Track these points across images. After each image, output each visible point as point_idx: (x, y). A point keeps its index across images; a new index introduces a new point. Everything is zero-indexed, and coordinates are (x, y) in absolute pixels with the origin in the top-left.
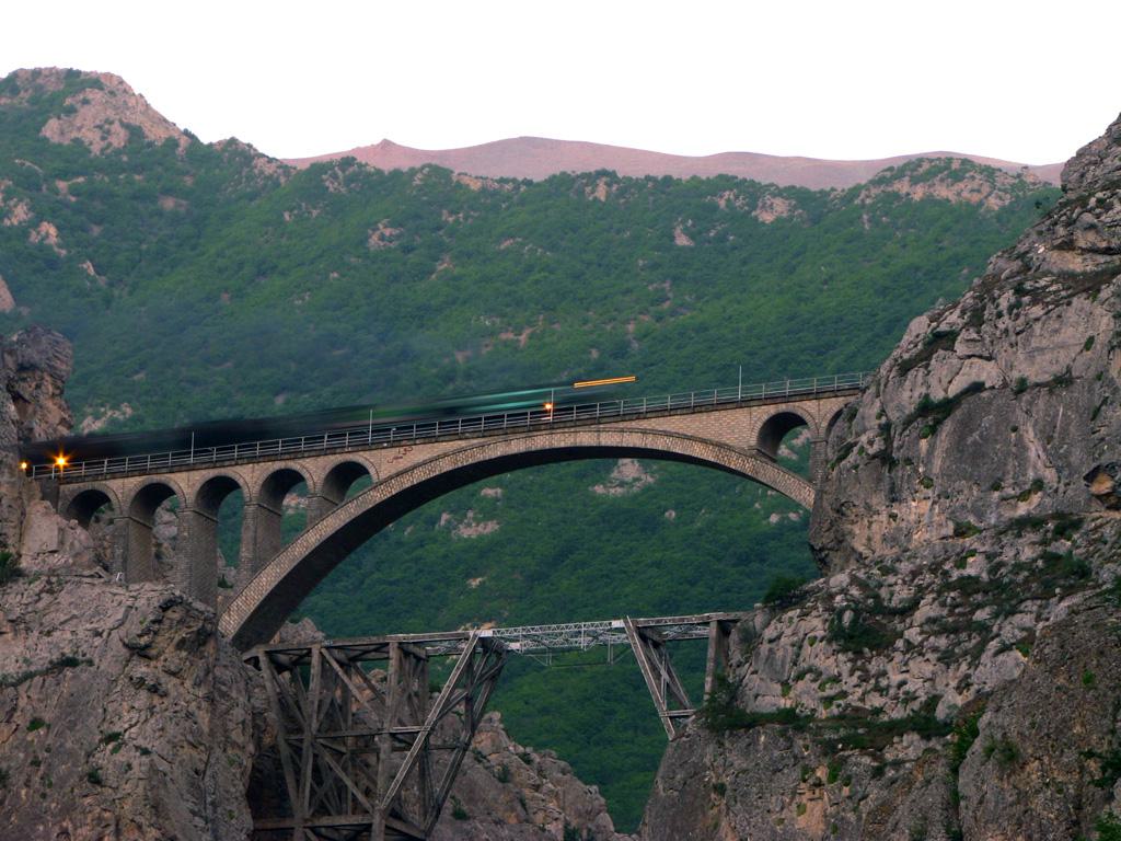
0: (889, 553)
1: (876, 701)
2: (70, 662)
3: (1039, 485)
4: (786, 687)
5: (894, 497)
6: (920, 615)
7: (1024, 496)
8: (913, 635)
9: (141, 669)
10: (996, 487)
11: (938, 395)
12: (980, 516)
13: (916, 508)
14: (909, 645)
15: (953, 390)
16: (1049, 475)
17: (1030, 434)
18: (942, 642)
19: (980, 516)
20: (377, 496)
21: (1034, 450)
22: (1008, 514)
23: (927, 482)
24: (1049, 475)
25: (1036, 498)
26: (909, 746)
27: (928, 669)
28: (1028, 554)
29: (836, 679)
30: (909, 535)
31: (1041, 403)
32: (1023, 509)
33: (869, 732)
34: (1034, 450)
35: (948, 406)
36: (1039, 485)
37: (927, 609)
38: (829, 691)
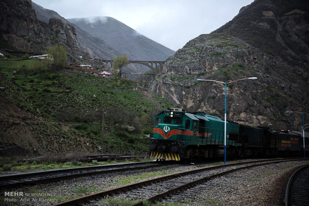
35: (174, 67)
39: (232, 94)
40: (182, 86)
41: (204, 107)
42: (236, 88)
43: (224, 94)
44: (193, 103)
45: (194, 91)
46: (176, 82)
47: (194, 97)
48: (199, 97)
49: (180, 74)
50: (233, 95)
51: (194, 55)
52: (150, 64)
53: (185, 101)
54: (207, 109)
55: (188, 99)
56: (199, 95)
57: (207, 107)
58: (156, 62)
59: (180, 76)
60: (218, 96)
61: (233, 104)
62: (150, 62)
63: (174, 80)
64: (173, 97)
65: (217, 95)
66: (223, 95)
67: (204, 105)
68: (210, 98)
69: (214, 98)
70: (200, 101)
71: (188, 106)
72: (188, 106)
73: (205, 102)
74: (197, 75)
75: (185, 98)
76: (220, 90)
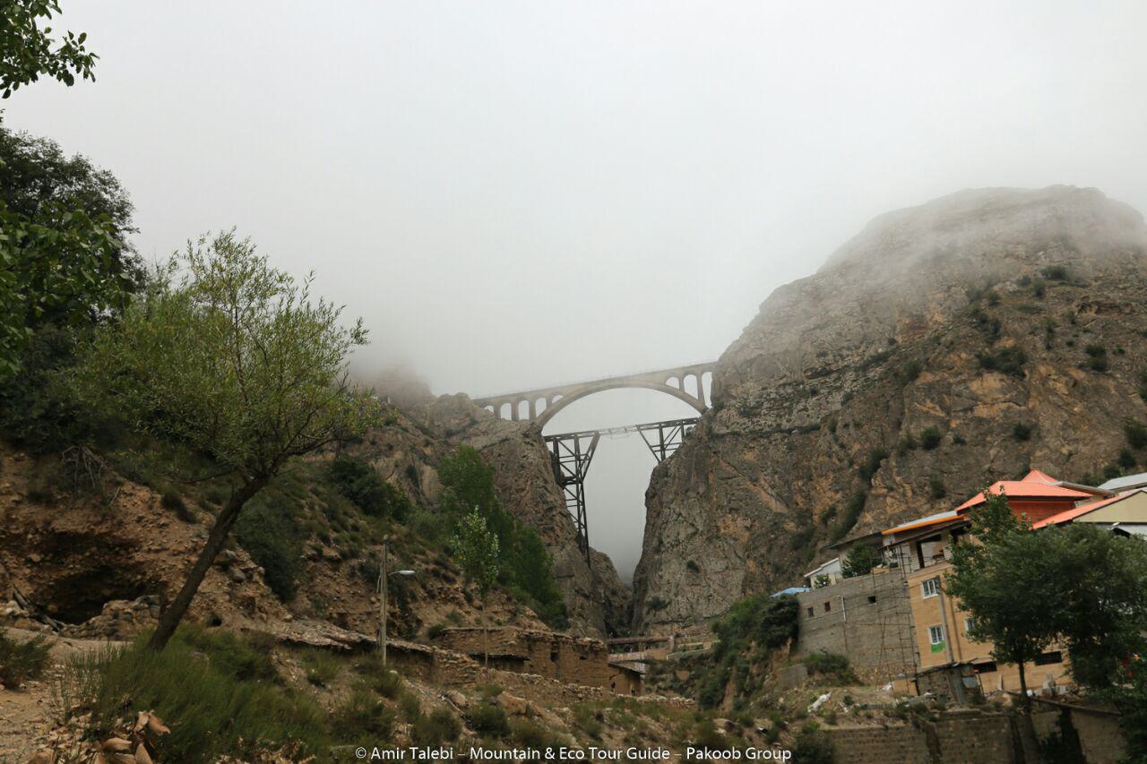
1: (757, 428)
2: (507, 439)
3: (785, 376)
4: (728, 427)
5: (742, 382)
7: (781, 379)
8: (765, 411)
9: (528, 440)
10: (772, 377)
12: (769, 384)
14: (765, 415)
15: (753, 356)
16: (788, 374)
18: (775, 412)
19: (769, 384)
24: (788, 374)
25: (784, 380)
26: (778, 436)
27: (773, 419)
28: (790, 391)
29: (744, 424)
32: (781, 382)
33: (758, 435)
37: (766, 405)
38: (744, 426)
39: (1025, 404)
40: (790, 431)
41: (889, 500)
42: (1043, 369)
43: (982, 411)
44: (837, 491)
46: (767, 421)
47: (835, 460)
49: (784, 385)
50: (1031, 411)
51: (834, 292)
52: (673, 382)
53: (800, 490)
54: (904, 507)
57: (904, 495)
59: (782, 391)
61: (1038, 454)
62: (670, 373)
63: (755, 415)
64: (755, 490)
65: (946, 424)
66: (980, 420)
68: (910, 445)
70: (867, 474)
73: (888, 469)
74: (856, 370)
75: (798, 478)
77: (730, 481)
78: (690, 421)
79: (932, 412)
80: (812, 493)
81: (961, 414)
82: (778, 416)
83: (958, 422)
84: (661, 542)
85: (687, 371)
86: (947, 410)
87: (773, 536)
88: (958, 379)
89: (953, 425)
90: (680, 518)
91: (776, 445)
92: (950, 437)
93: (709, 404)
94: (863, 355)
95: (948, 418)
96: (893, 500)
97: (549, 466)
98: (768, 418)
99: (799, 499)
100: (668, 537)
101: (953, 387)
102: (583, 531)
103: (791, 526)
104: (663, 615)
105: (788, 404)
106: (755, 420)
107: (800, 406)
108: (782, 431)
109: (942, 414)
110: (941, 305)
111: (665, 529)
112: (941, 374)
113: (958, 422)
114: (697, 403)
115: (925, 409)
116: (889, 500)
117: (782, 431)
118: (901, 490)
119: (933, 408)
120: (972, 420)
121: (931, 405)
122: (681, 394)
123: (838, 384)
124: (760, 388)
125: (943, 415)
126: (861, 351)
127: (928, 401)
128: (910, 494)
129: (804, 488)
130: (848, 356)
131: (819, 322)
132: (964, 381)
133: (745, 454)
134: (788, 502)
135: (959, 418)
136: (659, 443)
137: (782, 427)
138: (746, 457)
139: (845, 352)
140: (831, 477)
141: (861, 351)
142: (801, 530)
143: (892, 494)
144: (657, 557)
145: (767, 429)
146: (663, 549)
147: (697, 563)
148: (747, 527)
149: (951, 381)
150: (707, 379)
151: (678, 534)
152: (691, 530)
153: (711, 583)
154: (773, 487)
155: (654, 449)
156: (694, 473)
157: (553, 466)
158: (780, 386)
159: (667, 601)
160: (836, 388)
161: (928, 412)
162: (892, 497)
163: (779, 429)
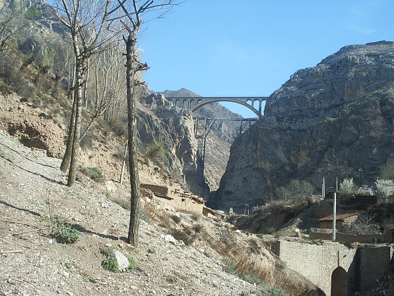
0: (278, 112)
1: (281, 127)
5: (278, 107)
6: (285, 119)
7: (294, 108)
10: (291, 106)
11: (282, 98)
13: (281, 108)
15: (284, 97)
16: (297, 106)
17: (295, 102)
18: (289, 121)
20: (204, 103)
21: (295, 103)
22: (292, 110)
23: (282, 105)
24: (297, 106)
25: (296, 108)
26: (289, 131)
30: (280, 111)
31: (296, 99)
32: (294, 109)
34: (295, 103)
36: (296, 107)
37: (286, 118)
40: (294, 130)
41: (329, 165)
45: (312, 133)
48: (320, 144)
52: (249, 102)
54: (335, 168)
55: (299, 151)
56: (320, 141)
57: (335, 163)
58: (259, 99)
60: (360, 140)
62: (249, 99)
65: (358, 137)
67: (328, 160)
69: (350, 144)
70: (322, 153)
71: (300, 165)
72: (300, 165)
75: (294, 150)
76: (365, 126)
77: (266, 147)
78: (253, 120)
79: (353, 131)
80: (299, 157)
81: (364, 134)
82: (291, 123)
83: (362, 137)
84: (234, 167)
85: (256, 99)
86: (359, 131)
87: (280, 172)
88: (366, 119)
89: (360, 138)
90: (243, 159)
91: (287, 135)
92: (358, 142)
93: (263, 114)
94: (329, 103)
95: (359, 135)
96: (331, 165)
97: (193, 129)
98: (286, 123)
99: (292, 158)
100: (237, 166)
101: (363, 122)
102: (203, 158)
103: (288, 168)
104: (230, 197)
105: (295, 119)
106: (280, 123)
107: (300, 120)
108: (291, 130)
109: (356, 133)
110: (365, 87)
111: (236, 162)
112: (359, 116)
113: (362, 137)
114: (258, 113)
115: (350, 130)
116: (329, 165)
117: (291, 130)
118: (335, 161)
119: (354, 130)
120: (368, 137)
121: (353, 128)
122: (252, 108)
123: (317, 114)
124: (285, 110)
125: (356, 133)
126: (329, 101)
127: (352, 126)
128: (338, 163)
129: (296, 154)
130: (323, 102)
131: (314, 87)
132: (368, 121)
133: (274, 137)
134: (289, 158)
135: (363, 135)
136: (239, 127)
137: (291, 128)
138: (274, 138)
139: (322, 101)
140: (308, 151)
141: (329, 101)
142: (292, 171)
143: (331, 162)
144: (231, 174)
145: (285, 128)
146: (234, 171)
147: (247, 178)
148: (270, 167)
149: (363, 119)
150: (264, 103)
151: (241, 165)
152: (246, 165)
153: (252, 187)
154: (284, 152)
155: (237, 129)
156: (252, 141)
157: (194, 130)
158: (293, 111)
159: (233, 192)
160: (316, 115)
161: (351, 131)
162: (331, 163)
163: (289, 128)
